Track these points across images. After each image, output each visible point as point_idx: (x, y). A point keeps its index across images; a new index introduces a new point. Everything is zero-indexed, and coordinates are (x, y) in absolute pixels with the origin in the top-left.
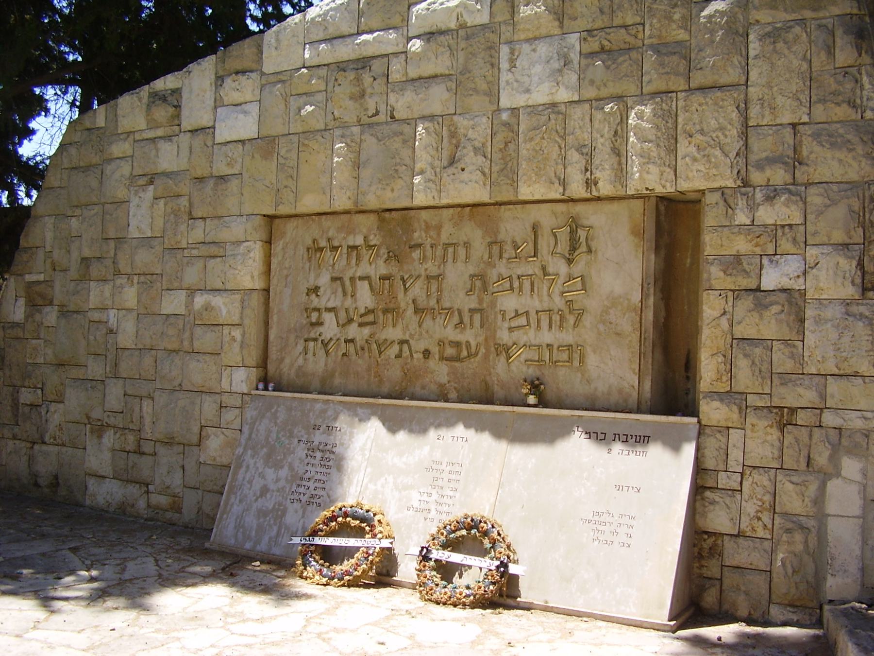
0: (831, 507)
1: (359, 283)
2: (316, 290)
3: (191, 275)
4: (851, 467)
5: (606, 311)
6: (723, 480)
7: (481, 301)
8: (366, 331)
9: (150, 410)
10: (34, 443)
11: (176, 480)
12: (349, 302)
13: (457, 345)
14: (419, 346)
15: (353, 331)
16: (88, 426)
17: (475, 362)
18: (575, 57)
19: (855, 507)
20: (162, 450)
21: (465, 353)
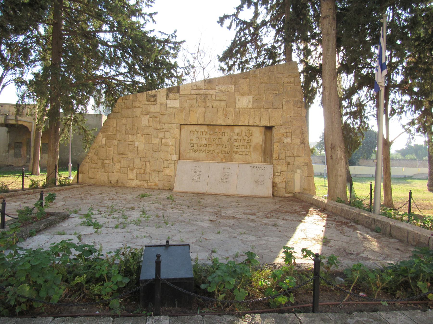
0: (295, 178)
1: (203, 139)
2: (192, 140)
3: (161, 135)
4: (299, 171)
6: (277, 174)
7: (230, 143)
8: (205, 148)
11: (156, 179)
13: (225, 151)
14: (217, 151)
18: (251, 100)
19: (299, 177)
20: (152, 173)
21: (227, 153)
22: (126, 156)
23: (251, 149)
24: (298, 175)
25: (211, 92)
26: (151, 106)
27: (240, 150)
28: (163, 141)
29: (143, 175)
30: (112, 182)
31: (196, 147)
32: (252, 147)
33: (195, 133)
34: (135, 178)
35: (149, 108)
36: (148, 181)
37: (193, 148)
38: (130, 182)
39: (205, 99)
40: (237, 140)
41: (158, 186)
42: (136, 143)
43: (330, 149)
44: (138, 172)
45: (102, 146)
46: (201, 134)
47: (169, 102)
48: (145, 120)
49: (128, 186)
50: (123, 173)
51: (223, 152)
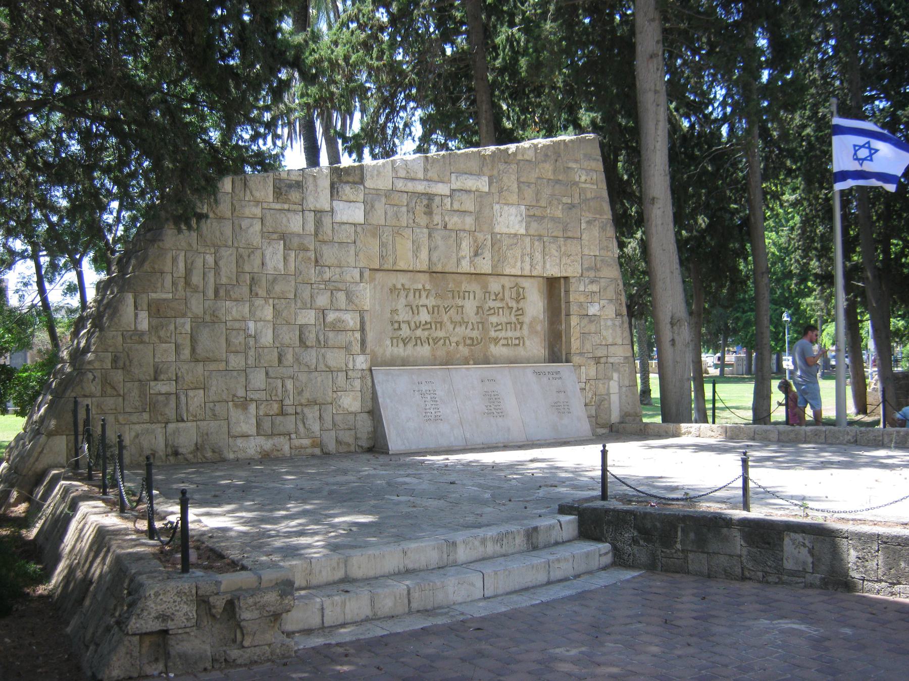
0: (611, 391)
3: (322, 300)
4: (615, 376)
5: (531, 323)
7: (482, 318)
8: (426, 333)
9: (292, 387)
10: (167, 423)
12: (416, 318)
13: (472, 339)
14: (454, 339)
15: (419, 332)
16: (231, 404)
17: (480, 346)
20: (306, 410)
21: (475, 342)
22: (222, 366)
23: (526, 331)
24: (614, 386)
25: (442, 189)
26: (290, 215)
27: (502, 334)
28: (331, 316)
29: (280, 418)
30: (181, 450)
31: (405, 332)
32: (525, 327)
33: (403, 294)
34: (254, 431)
35: (285, 220)
36: (293, 436)
37: (400, 332)
38: (240, 442)
39: (428, 206)
40: (494, 311)
41: (321, 445)
42: (251, 325)
43: (669, 326)
44: (261, 413)
45: (139, 337)
46: (417, 294)
47: (338, 205)
48: (274, 258)
49: (231, 456)
50: (215, 417)
51: (468, 342)
